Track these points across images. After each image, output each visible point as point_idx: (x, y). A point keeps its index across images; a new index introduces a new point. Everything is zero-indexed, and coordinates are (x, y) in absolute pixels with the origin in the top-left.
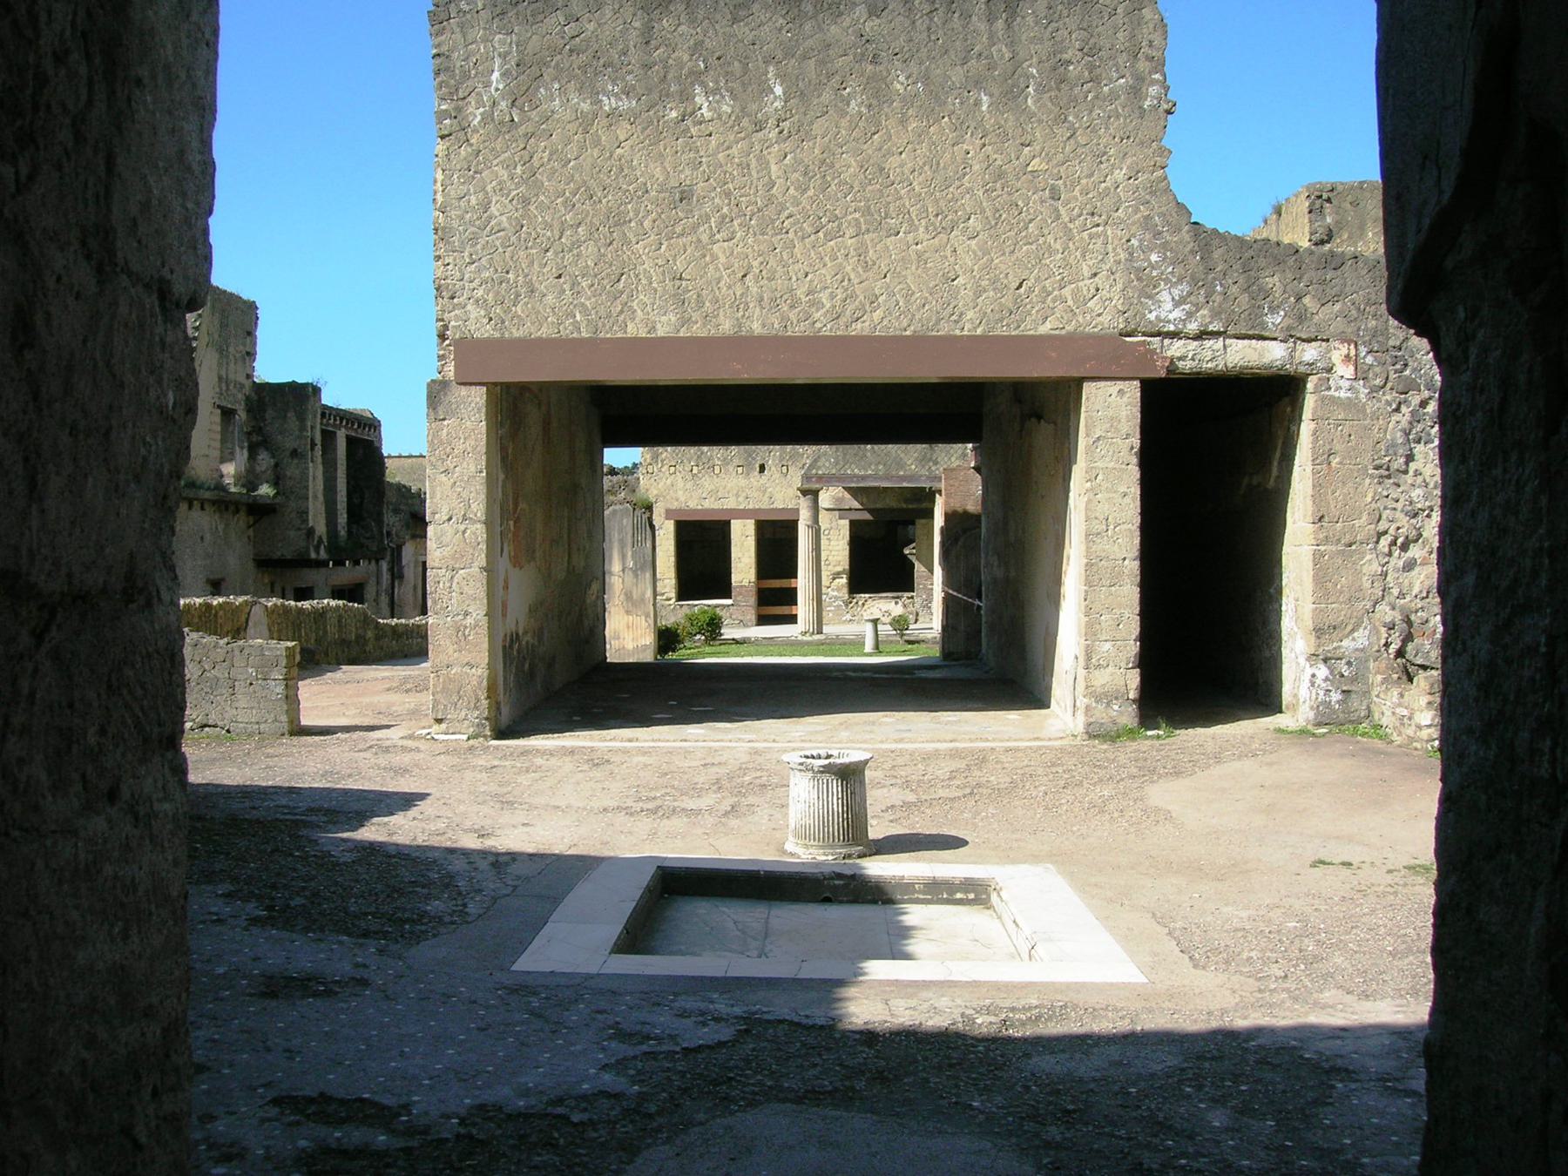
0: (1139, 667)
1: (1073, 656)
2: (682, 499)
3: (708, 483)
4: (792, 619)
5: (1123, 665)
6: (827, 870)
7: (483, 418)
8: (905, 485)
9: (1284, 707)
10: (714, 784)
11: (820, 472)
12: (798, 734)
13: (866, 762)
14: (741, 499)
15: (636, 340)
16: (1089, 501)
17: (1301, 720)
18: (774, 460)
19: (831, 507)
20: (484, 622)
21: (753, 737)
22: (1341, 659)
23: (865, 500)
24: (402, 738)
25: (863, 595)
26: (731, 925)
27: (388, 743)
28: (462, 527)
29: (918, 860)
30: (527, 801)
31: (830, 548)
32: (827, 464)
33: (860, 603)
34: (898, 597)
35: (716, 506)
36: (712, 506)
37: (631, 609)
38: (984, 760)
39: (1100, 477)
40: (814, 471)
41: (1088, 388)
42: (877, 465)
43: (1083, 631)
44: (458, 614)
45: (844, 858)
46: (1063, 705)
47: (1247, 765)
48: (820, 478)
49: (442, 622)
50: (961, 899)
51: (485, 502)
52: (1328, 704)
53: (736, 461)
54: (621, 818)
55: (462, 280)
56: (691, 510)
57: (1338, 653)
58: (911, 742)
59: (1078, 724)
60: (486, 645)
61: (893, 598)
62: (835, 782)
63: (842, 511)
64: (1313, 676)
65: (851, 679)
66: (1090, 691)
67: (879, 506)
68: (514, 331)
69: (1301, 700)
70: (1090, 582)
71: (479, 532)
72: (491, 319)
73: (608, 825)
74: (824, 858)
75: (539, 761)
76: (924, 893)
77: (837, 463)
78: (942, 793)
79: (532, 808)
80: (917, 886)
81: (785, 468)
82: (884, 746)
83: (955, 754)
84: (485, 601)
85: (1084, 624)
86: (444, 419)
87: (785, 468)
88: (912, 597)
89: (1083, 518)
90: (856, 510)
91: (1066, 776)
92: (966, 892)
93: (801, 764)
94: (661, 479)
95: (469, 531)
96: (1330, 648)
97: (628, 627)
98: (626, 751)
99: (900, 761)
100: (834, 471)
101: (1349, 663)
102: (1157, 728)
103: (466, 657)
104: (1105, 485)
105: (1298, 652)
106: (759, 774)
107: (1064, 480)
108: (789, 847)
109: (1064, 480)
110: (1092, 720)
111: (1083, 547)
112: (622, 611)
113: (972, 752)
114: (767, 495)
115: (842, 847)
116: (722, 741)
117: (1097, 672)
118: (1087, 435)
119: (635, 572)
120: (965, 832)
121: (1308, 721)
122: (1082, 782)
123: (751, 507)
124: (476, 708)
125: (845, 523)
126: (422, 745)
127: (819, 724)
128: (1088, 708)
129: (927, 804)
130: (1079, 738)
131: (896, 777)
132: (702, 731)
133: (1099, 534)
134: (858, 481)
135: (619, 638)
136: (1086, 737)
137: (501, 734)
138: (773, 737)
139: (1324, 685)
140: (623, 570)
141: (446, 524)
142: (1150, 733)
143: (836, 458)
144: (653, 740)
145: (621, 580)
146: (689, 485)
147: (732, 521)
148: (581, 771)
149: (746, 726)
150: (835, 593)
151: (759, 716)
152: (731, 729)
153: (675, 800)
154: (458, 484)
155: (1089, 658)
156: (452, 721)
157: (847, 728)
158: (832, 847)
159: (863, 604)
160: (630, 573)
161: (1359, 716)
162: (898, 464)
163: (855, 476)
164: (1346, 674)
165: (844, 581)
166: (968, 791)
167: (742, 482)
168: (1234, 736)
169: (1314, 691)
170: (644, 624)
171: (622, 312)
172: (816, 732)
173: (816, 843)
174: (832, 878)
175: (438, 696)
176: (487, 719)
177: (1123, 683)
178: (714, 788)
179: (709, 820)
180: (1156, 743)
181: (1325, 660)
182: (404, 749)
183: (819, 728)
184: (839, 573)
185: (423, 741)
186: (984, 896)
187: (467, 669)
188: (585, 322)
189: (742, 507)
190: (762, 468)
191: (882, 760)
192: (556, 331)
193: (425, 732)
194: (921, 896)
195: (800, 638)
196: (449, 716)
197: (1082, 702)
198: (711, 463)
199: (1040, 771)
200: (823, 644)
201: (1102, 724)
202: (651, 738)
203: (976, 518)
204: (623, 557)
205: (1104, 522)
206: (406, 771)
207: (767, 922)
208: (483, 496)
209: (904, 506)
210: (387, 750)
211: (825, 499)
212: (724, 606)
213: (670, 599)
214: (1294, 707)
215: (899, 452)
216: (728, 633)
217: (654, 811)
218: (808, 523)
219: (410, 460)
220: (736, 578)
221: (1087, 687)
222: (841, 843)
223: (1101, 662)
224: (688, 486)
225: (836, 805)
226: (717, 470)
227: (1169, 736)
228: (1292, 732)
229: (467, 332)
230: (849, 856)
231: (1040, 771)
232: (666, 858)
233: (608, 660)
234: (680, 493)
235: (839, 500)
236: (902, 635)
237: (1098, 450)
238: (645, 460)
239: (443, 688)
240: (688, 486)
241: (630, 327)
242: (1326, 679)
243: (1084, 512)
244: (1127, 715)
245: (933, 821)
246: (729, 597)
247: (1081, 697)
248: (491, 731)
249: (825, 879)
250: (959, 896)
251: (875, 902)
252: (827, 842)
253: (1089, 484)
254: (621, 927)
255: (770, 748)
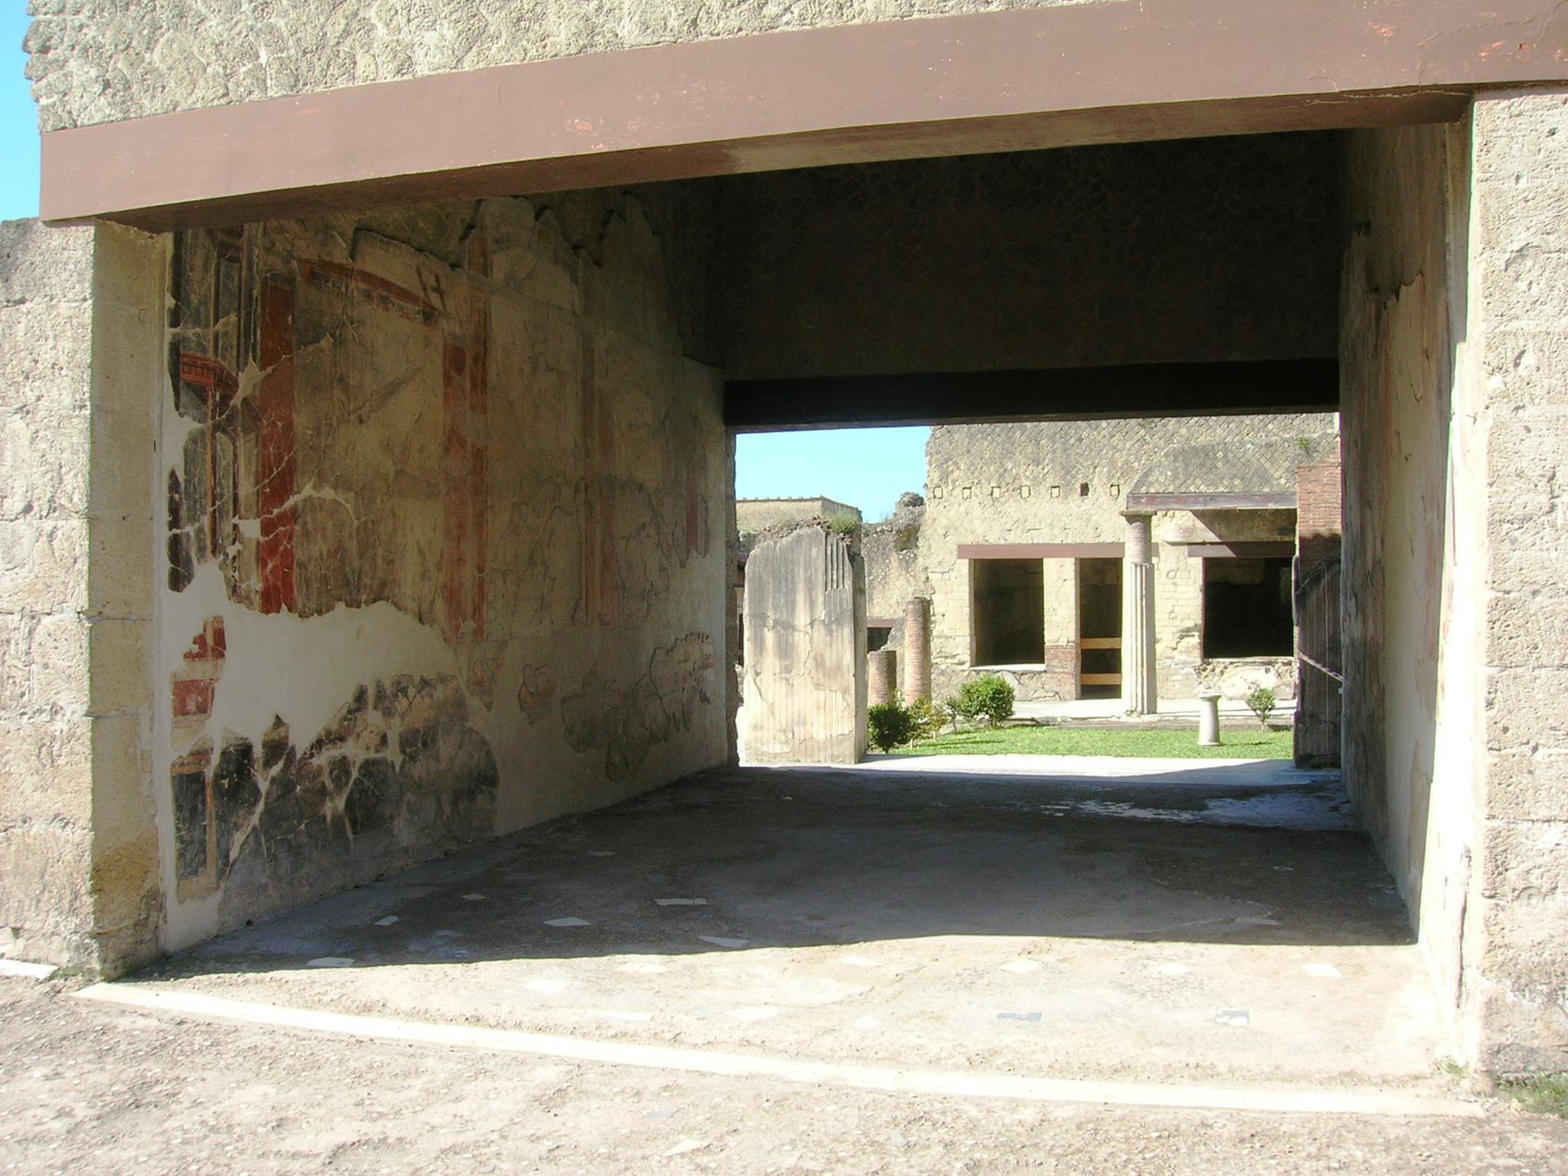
2: (979, 531)
3: (1013, 508)
4: (1113, 691)
7: (87, 293)
8: (1271, 506)
11: (1152, 490)
14: (1056, 531)
15: (375, 92)
16: (1498, 429)
18: (1100, 478)
19: (1179, 540)
20: (85, 728)
23: (1224, 530)
25: (1221, 660)
28: (48, 525)
31: (1177, 596)
32: (1162, 479)
33: (1218, 671)
34: (1269, 663)
35: (1025, 539)
36: (1018, 541)
37: (822, 681)
39: (1528, 360)
40: (1143, 490)
41: (1487, 116)
42: (1232, 479)
43: (1484, 790)
44: (40, 711)
48: (1152, 498)
49: (13, 727)
51: (86, 470)
53: (1050, 481)
55: (61, 11)
56: (991, 545)
60: (87, 779)
61: (1263, 664)
63: (1193, 545)
65: (1050, 824)
67: (1242, 539)
68: (146, 102)
70: (1499, 658)
71: (75, 534)
72: (107, 85)
77: (1175, 477)
81: (1114, 489)
84: (86, 684)
85: (1483, 775)
86: (22, 301)
87: (1114, 489)
88: (1289, 663)
89: (1483, 477)
90: (1212, 544)
94: (952, 505)
95: (59, 533)
97: (818, 709)
100: (1171, 489)
103: (54, 802)
104: (1543, 382)
107: (1440, 394)
109: (1440, 394)
110: (1502, 1039)
111: (1484, 559)
112: (810, 685)
114: (1092, 524)
117: (1520, 909)
118: (1489, 245)
119: (828, 626)
123: (1069, 541)
124: (73, 911)
125: (1197, 564)
133: (1528, 519)
134: (1206, 503)
135: (805, 724)
136: (1484, 1084)
140: (812, 624)
141: (22, 520)
143: (1174, 471)
145: (808, 638)
146: (989, 512)
147: (1045, 560)
150: (1184, 657)
154: (41, 434)
155: (1498, 867)
159: (1222, 673)
160: (821, 627)
162: (1262, 477)
163: (1201, 495)
165: (1195, 640)
167: (1058, 507)
170: (841, 704)
171: (347, 32)
184: (1188, 630)
187: (56, 827)
188: (276, 66)
189: (1058, 541)
190: (1085, 490)
192: (221, 91)
195: (1124, 719)
198: (1017, 485)
200: (1152, 729)
201: (1532, 1050)
203: (1334, 540)
204: (812, 604)
205: (1543, 483)
208: (83, 458)
209: (1279, 538)
211: (1166, 528)
212: (1034, 673)
213: (963, 663)
215: (1263, 461)
216: (1020, 710)
218: (1138, 560)
219: (767, 504)
220: (1050, 636)
221: (1491, 948)
223: (1533, 879)
224: (987, 514)
226: (1025, 491)
229: (65, 115)
233: (742, 764)
234: (977, 523)
235: (1189, 531)
236: (1264, 718)
237: (1522, 285)
238: (932, 480)
240: (987, 514)
241: (363, 60)
243: (1483, 458)
246: (1042, 661)
253: (1498, 378)
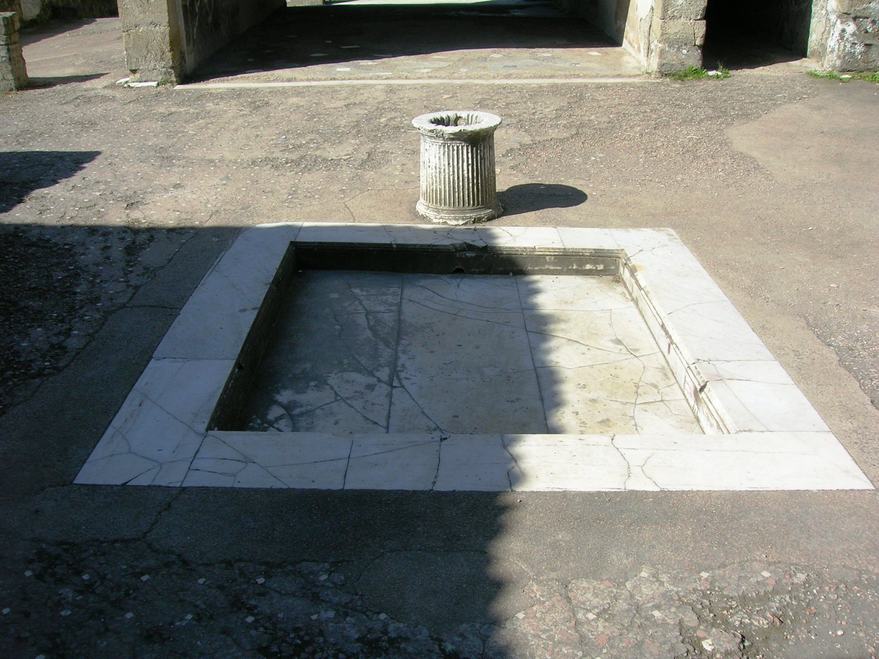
0: (704, 18)
1: (649, 8)
5: (693, 17)
6: (458, 240)
9: (808, 53)
10: (353, 127)
12: (426, 71)
13: (495, 128)
17: (826, 65)
21: (389, 74)
22: (867, 18)
24: (105, 87)
26: (362, 320)
27: (92, 93)
29: (544, 223)
30: (186, 155)
38: (581, 97)
45: (474, 222)
46: (636, 46)
47: (797, 108)
50: (591, 270)
52: (852, 55)
54: (267, 171)
57: (866, 14)
58: (519, 77)
59: (654, 64)
62: (465, 148)
64: (843, 31)
66: (665, 38)
69: (829, 50)
73: (253, 182)
74: (454, 223)
75: (210, 106)
76: (555, 264)
78: (553, 133)
79: (190, 162)
80: (547, 258)
82: (497, 82)
83: (556, 90)
91: (655, 116)
92: (595, 263)
93: (432, 131)
96: (861, 8)
98: (283, 92)
99: (512, 98)
101: (874, 22)
102: (716, 68)
105: (829, 11)
106: (393, 114)
108: (421, 208)
110: (664, 62)
113: (569, 88)
115: (472, 211)
116: (364, 78)
117: (671, 23)
120: (582, 182)
121: (834, 67)
122: (668, 122)
124: (162, 59)
126: (118, 94)
127: (441, 60)
128: (662, 52)
129: (541, 147)
130: (653, 76)
131: (510, 116)
132: (348, 69)
136: (658, 75)
137: (185, 78)
138: (405, 74)
139: (851, 39)
142: (711, 73)
144: (308, 80)
148: (243, 115)
149: (384, 63)
151: (395, 54)
152: (371, 66)
153: (318, 148)
155: (665, 10)
156: (143, 71)
157: (464, 64)
158: (462, 211)
161: (875, 66)
164: (870, 31)
166: (574, 131)
168: (778, 78)
169: (843, 43)
172: (440, 69)
173: (447, 208)
174: (464, 250)
175: (130, 52)
176: (172, 68)
177: (691, 32)
178: (354, 132)
179: (347, 173)
180: (719, 83)
181: (855, 19)
182: (105, 99)
183: (442, 64)
185: (121, 90)
186: (613, 268)
187: (152, 28)
191: (497, 97)
193: (123, 80)
194: (552, 268)
196: (141, 68)
197: (656, 45)
199: (631, 110)
201: (672, 65)
202: (306, 77)
206: (93, 124)
207: (400, 312)
210: (89, 100)
214: (820, 55)
217: (297, 163)
221: (662, 35)
222: (471, 207)
225: (466, 171)
227: (725, 77)
228: (822, 77)
230: (478, 220)
231: (631, 110)
232: (300, 229)
239: (134, 44)
242: (853, 34)
244: (694, 58)
245: (549, 167)
247: (656, 42)
248: (176, 77)
249: (456, 252)
250: (588, 267)
251: (505, 273)
252: (455, 204)
254: (233, 363)
255: (403, 86)
